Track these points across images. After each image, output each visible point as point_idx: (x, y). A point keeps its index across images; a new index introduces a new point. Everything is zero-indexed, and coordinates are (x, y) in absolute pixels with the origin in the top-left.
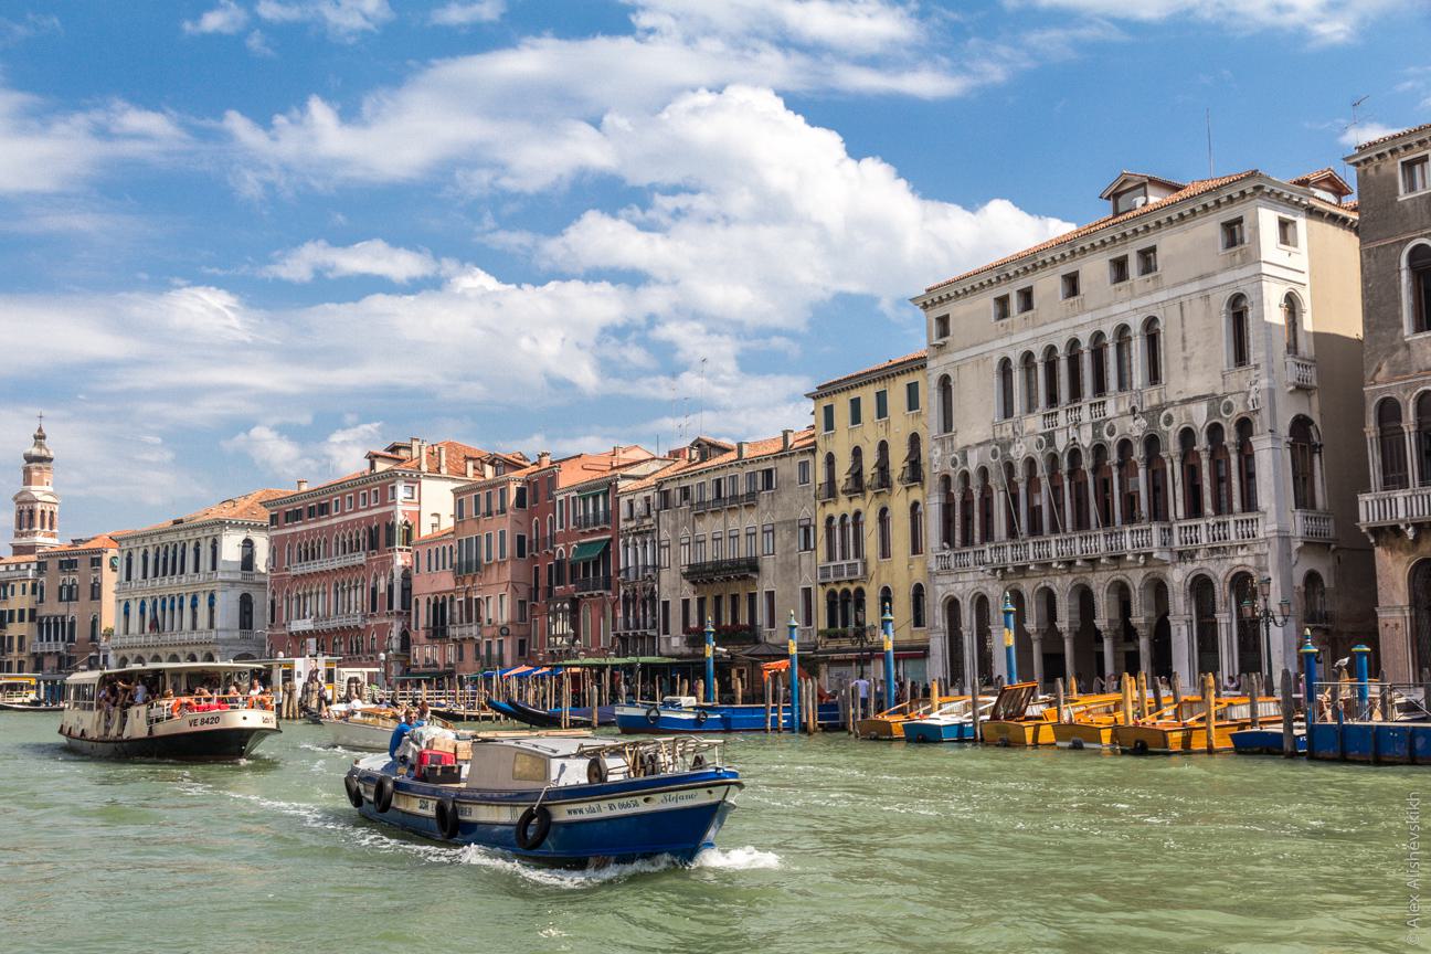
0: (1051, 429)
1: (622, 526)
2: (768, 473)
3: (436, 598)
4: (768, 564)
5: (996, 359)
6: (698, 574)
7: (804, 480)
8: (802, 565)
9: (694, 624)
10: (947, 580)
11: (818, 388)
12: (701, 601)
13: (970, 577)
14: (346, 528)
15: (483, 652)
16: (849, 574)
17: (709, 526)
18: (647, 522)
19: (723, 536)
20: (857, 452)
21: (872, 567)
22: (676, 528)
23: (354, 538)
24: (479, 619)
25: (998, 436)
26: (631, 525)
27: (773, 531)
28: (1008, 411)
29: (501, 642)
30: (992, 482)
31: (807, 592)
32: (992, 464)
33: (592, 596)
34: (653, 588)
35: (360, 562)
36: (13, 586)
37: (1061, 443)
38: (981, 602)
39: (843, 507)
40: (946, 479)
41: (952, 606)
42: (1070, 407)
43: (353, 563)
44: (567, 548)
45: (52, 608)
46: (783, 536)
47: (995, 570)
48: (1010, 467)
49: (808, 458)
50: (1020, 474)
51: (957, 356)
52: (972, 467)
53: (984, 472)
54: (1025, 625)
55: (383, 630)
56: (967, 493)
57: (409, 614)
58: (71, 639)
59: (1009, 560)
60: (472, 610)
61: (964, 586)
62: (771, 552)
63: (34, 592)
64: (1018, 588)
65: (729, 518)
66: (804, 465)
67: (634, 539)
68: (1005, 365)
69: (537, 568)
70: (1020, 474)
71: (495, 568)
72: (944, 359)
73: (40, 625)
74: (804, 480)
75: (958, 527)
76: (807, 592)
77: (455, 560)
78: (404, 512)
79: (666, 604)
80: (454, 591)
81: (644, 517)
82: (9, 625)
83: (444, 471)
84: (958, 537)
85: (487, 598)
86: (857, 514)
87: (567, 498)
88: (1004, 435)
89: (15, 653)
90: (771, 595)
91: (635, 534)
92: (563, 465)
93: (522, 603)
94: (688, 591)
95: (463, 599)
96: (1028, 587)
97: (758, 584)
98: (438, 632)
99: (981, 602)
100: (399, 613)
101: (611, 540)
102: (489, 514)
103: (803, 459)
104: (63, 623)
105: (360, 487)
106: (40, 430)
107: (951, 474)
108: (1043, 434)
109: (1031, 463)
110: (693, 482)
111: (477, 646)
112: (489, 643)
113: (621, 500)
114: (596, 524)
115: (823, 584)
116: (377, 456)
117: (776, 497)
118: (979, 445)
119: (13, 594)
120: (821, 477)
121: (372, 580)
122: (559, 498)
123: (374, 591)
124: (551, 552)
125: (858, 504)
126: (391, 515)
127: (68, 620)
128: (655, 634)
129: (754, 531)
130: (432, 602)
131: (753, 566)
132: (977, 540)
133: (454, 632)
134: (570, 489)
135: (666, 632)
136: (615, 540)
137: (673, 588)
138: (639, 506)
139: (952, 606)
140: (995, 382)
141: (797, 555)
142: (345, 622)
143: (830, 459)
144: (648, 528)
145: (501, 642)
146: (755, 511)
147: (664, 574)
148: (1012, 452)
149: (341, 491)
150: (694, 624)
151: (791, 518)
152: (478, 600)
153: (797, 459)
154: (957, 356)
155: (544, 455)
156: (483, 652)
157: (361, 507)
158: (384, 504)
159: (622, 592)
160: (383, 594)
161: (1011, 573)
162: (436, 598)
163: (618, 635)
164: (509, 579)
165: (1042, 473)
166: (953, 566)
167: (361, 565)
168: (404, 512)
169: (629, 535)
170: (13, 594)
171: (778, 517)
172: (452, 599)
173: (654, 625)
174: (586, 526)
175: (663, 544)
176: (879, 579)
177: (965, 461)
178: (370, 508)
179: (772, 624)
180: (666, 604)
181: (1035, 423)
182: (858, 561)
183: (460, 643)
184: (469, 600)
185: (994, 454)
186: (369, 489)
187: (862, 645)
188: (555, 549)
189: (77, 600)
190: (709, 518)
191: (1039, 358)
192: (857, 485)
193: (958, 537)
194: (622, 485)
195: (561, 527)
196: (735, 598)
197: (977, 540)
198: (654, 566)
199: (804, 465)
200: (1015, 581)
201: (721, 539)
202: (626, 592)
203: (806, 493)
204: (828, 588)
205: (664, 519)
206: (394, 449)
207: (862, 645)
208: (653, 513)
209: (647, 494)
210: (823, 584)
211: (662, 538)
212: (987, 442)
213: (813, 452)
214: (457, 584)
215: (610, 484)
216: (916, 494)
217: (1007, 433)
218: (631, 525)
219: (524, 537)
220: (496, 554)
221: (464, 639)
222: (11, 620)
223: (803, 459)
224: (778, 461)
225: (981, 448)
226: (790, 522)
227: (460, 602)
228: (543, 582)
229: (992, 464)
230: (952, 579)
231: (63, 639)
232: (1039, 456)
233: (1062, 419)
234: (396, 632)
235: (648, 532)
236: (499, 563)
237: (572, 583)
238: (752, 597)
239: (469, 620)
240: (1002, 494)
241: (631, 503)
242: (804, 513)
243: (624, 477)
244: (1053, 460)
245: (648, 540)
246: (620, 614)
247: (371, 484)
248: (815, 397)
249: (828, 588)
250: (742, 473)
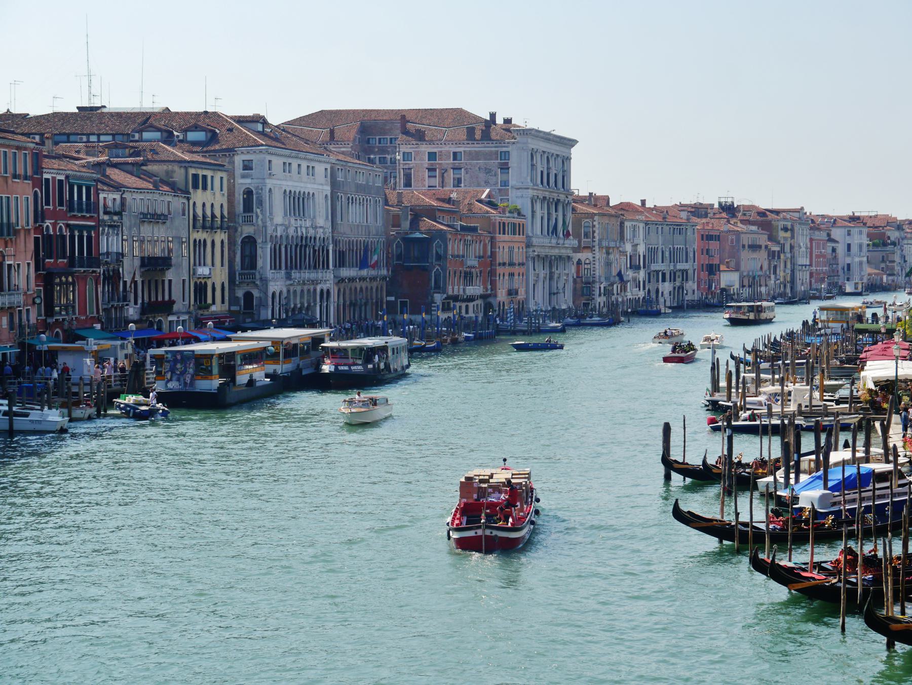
12: (143, 282)
29: (28, 310)
31: (184, 280)
68: (285, 191)
71: (22, 234)
87: (54, 178)
90: (170, 281)
102: (15, 176)
114: (80, 210)
122: (46, 176)
137: (129, 270)
152: (10, 266)
196: (156, 281)
236: (25, 230)
238: (163, 281)
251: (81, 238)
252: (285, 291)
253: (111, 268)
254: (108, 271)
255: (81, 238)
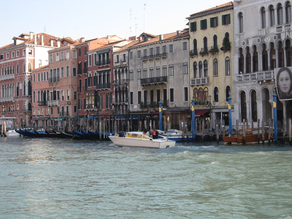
0: (279, 32)
1: (115, 65)
2: (171, 46)
3: (42, 91)
4: (171, 79)
5: (259, 8)
6: (144, 82)
7: (185, 48)
8: (184, 79)
9: (143, 100)
10: (241, 85)
11: (191, 16)
12: (145, 92)
13: (249, 84)
14: (6, 65)
15: (61, 110)
16: (202, 82)
17: (148, 65)
18: (124, 63)
19: (153, 68)
20: (205, 39)
21: (211, 80)
22: (135, 66)
23: (9, 69)
24: (59, 99)
25: (260, 34)
26: (118, 64)
27: (173, 67)
28: (263, 26)
29: (67, 107)
30: (257, 51)
31: (186, 89)
32: (258, 44)
33: (103, 90)
34: (127, 88)
35: (12, 78)
37: (283, 38)
38: (253, 93)
39: (199, 59)
40: (241, 49)
41: (243, 94)
42: (287, 25)
43: (10, 78)
44: (93, 73)
46: (177, 69)
47: (259, 82)
48: (264, 45)
49: (187, 41)
50: (268, 48)
51: (245, 6)
52: (251, 45)
53: (255, 47)
54: (269, 101)
55: (21, 103)
56: (248, 54)
57: (31, 97)
59: (264, 78)
60: (55, 96)
61: (247, 88)
62: (172, 74)
64: (267, 87)
65: (156, 62)
66: (185, 43)
67: (119, 70)
69: (80, 80)
70: (268, 48)
72: (241, 7)
74: (185, 48)
75: (245, 66)
76: (186, 89)
77: (49, 77)
78: (29, 60)
79: (132, 93)
80: (49, 88)
81: (123, 62)
83: (43, 44)
84: (245, 70)
85: (62, 91)
86: (205, 61)
87: (93, 54)
88: (262, 34)
90: (172, 90)
91: (119, 68)
92: (90, 42)
93: (75, 93)
94: (140, 89)
95: (52, 91)
96: (270, 87)
97: (167, 86)
98: (44, 103)
99: (253, 93)
100: (27, 96)
101: (110, 70)
103: (185, 41)
105: (12, 50)
107: (243, 48)
108: (277, 34)
109: (272, 44)
110: (142, 49)
111: (58, 109)
112: (63, 108)
113: (114, 55)
115: (192, 86)
116: (17, 39)
117: (174, 55)
118: (254, 37)
120: (192, 48)
121: (17, 85)
122: (89, 54)
123: (18, 88)
124: (86, 74)
125: (206, 58)
126: (23, 62)
128: (128, 104)
129: (186, 64)
130: (44, 92)
131: (165, 79)
132: (252, 71)
133: (49, 103)
134: (93, 51)
135: (132, 103)
136: (112, 70)
137: (135, 87)
138: (121, 57)
139: (243, 94)
140: (259, 15)
141: (182, 76)
142: (7, 100)
143: (195, 42)
144: (124, 66)
145: (67, 107)
146: (166, 60)
147: (131, 83)
148: (265, 40)
149: (4, 52)
150: (143, 100)
151: (180, 62)
152: (58, 92)
153: (182, 41)
154: (245, 6)
155: (82, 38)
156: (61, 110)
157: (12, 57)
158: (21, 56)
159: (114, 89)
160: (22, 90)
161: (265, 83)
162: (42, 91)
163: (113, 104)
164: (70, 84)
165: (276, 47)
166: (243, 80)
167: (13, 79)
168: (29, 60)
169: (117, 68)
171: (175, 62)
172: (48, 91)
173: (127, 101)
174: (100, 65)
175: (130, 71)
176: (213, 85)
177: (248, 43)
178: (15, 58)
179: (172, 100)
180: (132, 93)
181: (274, 30)
182: (206, 78)
183: (52, 107)
184: (55, 92)
185: (259, 40)
186: (15, 51)
187: (210, 107)
188: (88, 73)
190: (148, 62)
191: (275, 7)
192: (205, 52)
193: (245, 70)
194: (115, 50)
195: (90, 65)
196: (158, 91)
197: (252, 71)
198: (127, 80)
199: (185, 43)
200: (265, 85)
201: (153, 70)
202: (116, 89)
203: (186, 53)
204: (194, 87)
205: (131, 62)
206: (22, 36)
207: (210, 107)
208: (127, 60)
209: (124, 53)
210: (192, 86)
211: (130, 69)
212: (256, 36)
213: (189, 39)
214: (50, 86)
215: (110, 50)
216: (227, 54)
217: (263, 33)
218: (118, 64)
219: (75, 69)
220: (65, 75)
221: (53, 106)
223: (185, 41)
224: (175, 42)
225: (254, 39)
226: (180, 64)
227: (51, 92)
228: (83, 85)
229: (258, 44)
230: (243, 84)
232: (275, 42)
233: (283, 29)
234: (26, 104)
235: (124, 67)
237: (95, 85)
238: (165, 91)
239: (55, 99)
240: (261, 55)
241: (118, 56)
242: (186, 60)
243: (115, 47)
244: (280, 43)
245: (125, 70)
246: (114, 97)
247: (16, 49)
248: (189, 19)
249: (194, 87)
250: (161, 46)
251: (104, 76)
252: (258, 89)
253: (121, 87)
254: (120, 88)
255: (104, 76)
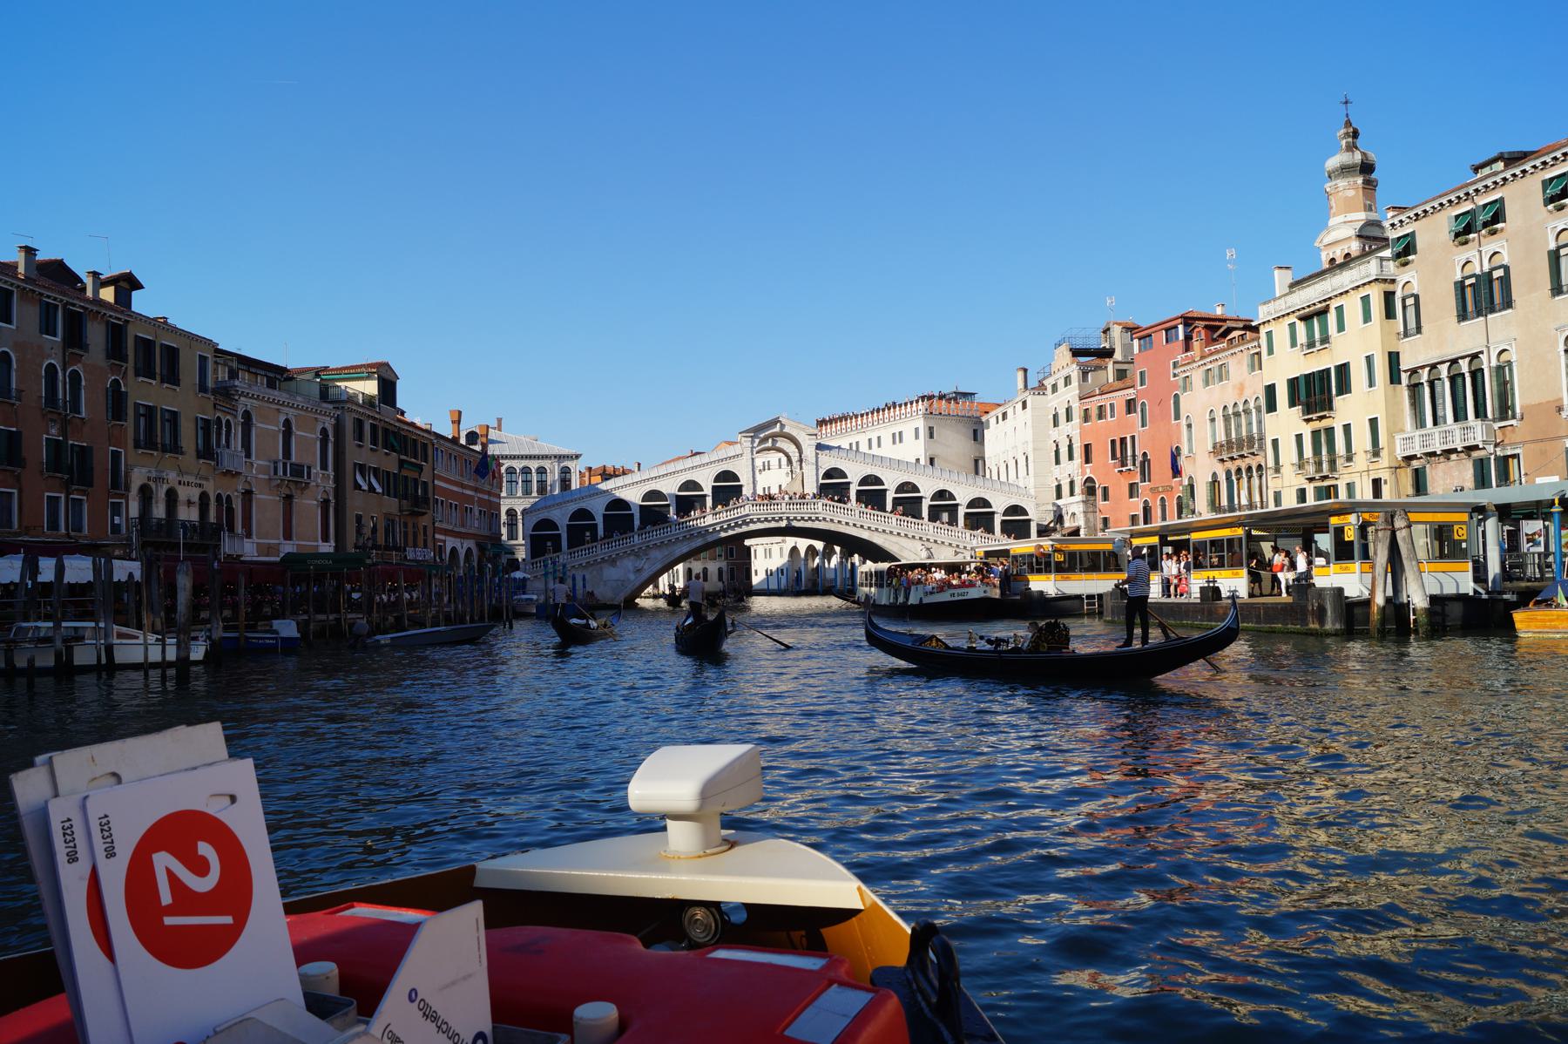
36: (1340, 309)
45: (1445, 338)
58: (1505, 409)
63: (1390, 313)
73: (1415, 388)
82: (1338, 402)
89: (1361, 460)
104: (1477, 374)
106: (1348, 124)
119: (1341, 328)
127: (1488, 363)
170: (1341, 328)
189: (1508, 303)
222: (1344, 388)
231: (1480, 413)
